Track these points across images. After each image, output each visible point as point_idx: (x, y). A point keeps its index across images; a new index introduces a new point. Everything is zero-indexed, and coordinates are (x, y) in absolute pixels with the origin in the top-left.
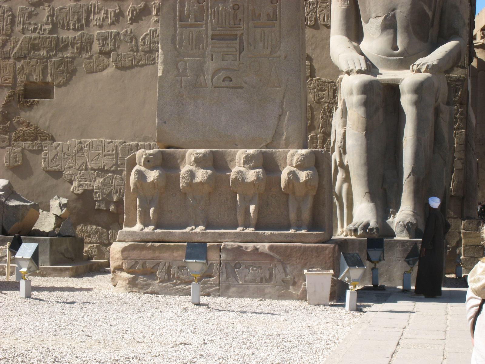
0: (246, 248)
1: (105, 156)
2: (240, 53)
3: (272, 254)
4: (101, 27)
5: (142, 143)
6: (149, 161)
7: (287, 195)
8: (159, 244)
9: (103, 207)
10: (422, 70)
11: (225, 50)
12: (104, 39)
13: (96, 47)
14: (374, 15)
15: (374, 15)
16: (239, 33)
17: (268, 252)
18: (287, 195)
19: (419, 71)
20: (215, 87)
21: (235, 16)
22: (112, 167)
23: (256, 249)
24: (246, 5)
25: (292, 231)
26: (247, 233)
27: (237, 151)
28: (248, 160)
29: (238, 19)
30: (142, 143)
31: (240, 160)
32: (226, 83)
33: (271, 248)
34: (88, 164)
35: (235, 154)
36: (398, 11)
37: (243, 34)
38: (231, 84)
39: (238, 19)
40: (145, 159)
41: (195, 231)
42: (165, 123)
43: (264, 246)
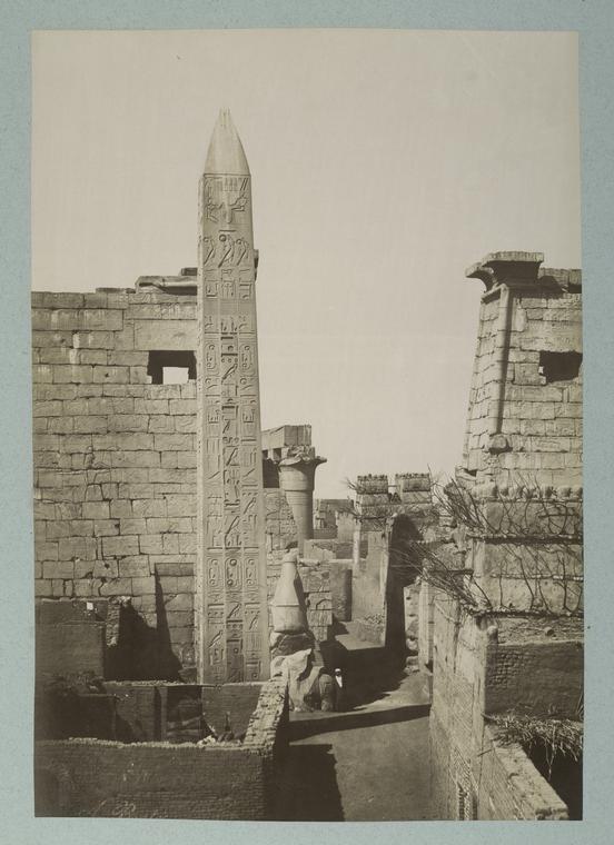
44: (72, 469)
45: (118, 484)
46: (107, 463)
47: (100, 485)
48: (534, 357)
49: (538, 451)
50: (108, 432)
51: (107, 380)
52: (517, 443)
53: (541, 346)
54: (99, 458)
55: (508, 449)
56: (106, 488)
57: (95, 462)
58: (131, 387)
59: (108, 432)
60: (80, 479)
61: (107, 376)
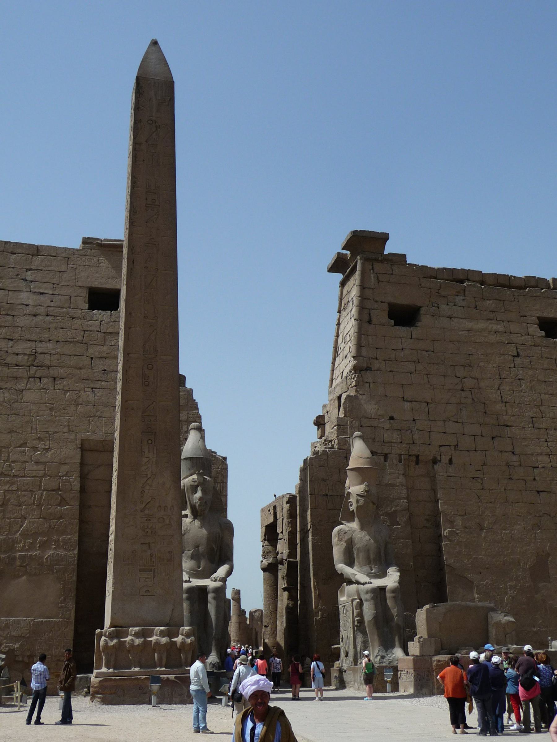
0: (164, 678)
1: (22, 628)
2: (154, 578)
3: (177, 680)
4: (20, 551)
5: (45, 620)
6: (110, 634)
7: (181, 650)
8: (119, 678)
9: (21, 659)
10: (217, 580)
11: (146, 576)
12: (23, 558)
13: (18, 563)
14: (187, 549)
15: (187, 549)
16: (153, 568)
17: (174, 679)
18: (181, 650)
19: (215, 581)
20: (141, 596)
21: (151, 559)
22: (26, 635)
23: (168, 678)
24: (157, 554)
25: (158, 669)
26: (161, 670)
27: (155, 629)
28: (161, 632)
29: (153, 561)
30: (45, 620)
31: (157, 632)
32: (147, 594)
33: (176, 677)
34: (12, 633)
35: (153, 630)
36: (200, 548)
37: (155, 568)
38: (149, 594)
39: (153, 561)
40: (109, 633)
41: (135, 670)
42: (115, 614)
43: (172, 677)
44: (17, 365)
45: (55, 379)
46: (48, 363)
47: (40, 378)
48: (386, 307)
49: (390, 371)
50: (50, 340)
51: (52, 304)
52: (376, 365)
53: (390, 299)
54: (40, 357)
55: (368, 369)
56: (45, 380)
57: (37, 361)
58: (71, 310)
59: (50, 340)
60: (20, 372)
61: (52, 301)
